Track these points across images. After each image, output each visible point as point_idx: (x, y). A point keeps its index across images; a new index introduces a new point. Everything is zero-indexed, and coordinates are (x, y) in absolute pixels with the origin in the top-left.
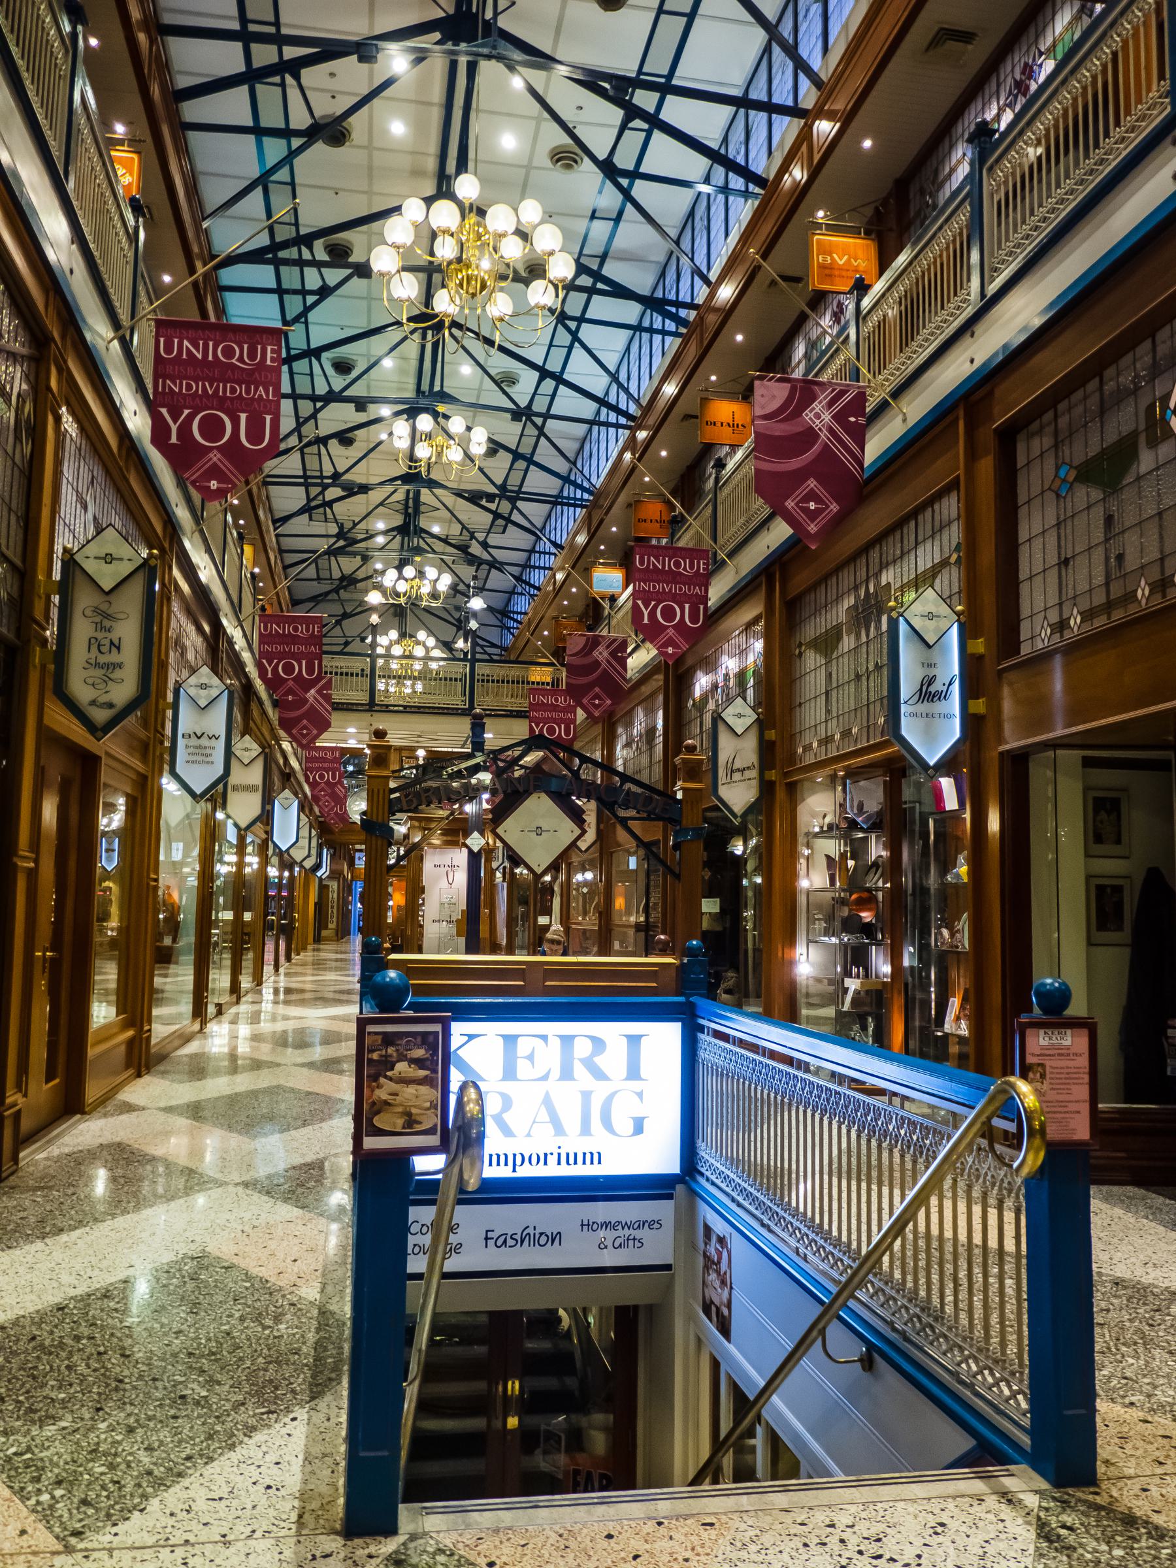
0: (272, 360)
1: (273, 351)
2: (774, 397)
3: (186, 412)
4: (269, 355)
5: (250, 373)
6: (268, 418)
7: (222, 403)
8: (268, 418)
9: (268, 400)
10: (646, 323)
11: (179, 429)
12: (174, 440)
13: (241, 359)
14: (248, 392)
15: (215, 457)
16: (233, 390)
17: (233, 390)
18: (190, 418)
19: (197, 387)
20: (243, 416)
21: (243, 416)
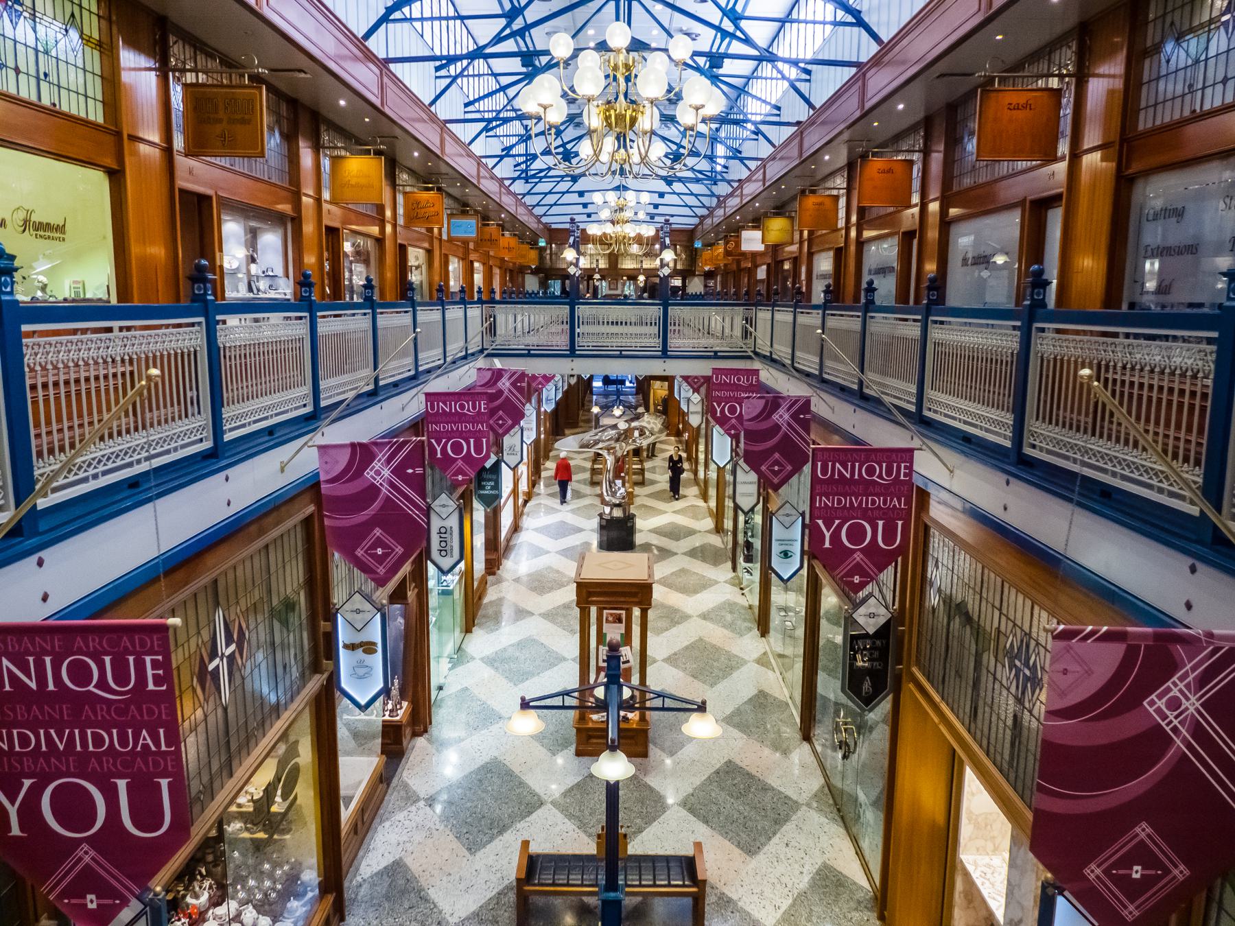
0: (158, 680)
1: (155, 665)
2: (1089, 673)
3: (27, 783)
4: (150, 672)
5: (121, 708)
7: (83, 764)
9: (159, 753)
11: (19, 812)
12: (16, 831)
13: (103, 684)
14: (123, 741)
16: (98, 741)
17: (98, 741)
18: (35, 792)
19: (38, 739)
20: (122, 784)
21: (122, 784)
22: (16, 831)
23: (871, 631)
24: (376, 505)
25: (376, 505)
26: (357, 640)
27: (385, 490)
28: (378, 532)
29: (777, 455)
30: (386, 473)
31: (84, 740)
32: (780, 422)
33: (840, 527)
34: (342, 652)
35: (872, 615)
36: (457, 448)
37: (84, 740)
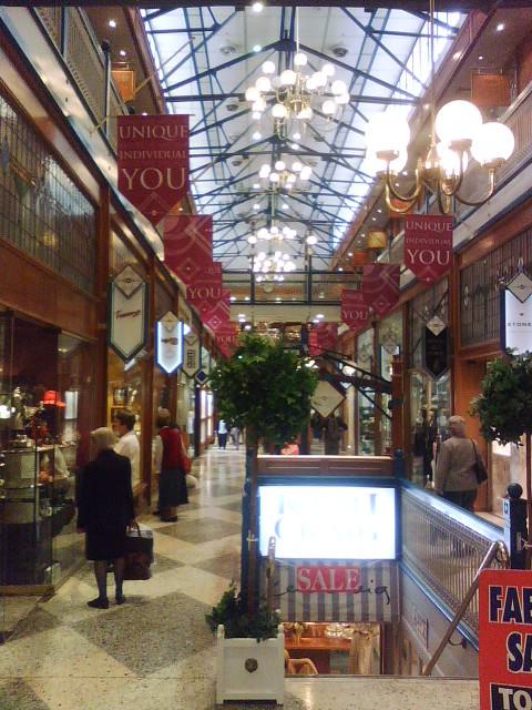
6: (183, 169)
8: (183, 169)
10: (424, 31)
12: (130, 187)
13: (166, 135)
14: (171, 154)
15: (154, 195)
22: (130, 187)
23: (436, 334)
24: (189, 246)
25: (189, 246)
26: (168, 338)
27: (194, 238)
28: (189, 259)
29: (382, 296)
30: (195, 230)
31: (158, 154)
32: (384, 278)
33: (418, 253)
34: (160, 345)
35: (436, 325)
36: (203, 293)
37: (158, 154)
